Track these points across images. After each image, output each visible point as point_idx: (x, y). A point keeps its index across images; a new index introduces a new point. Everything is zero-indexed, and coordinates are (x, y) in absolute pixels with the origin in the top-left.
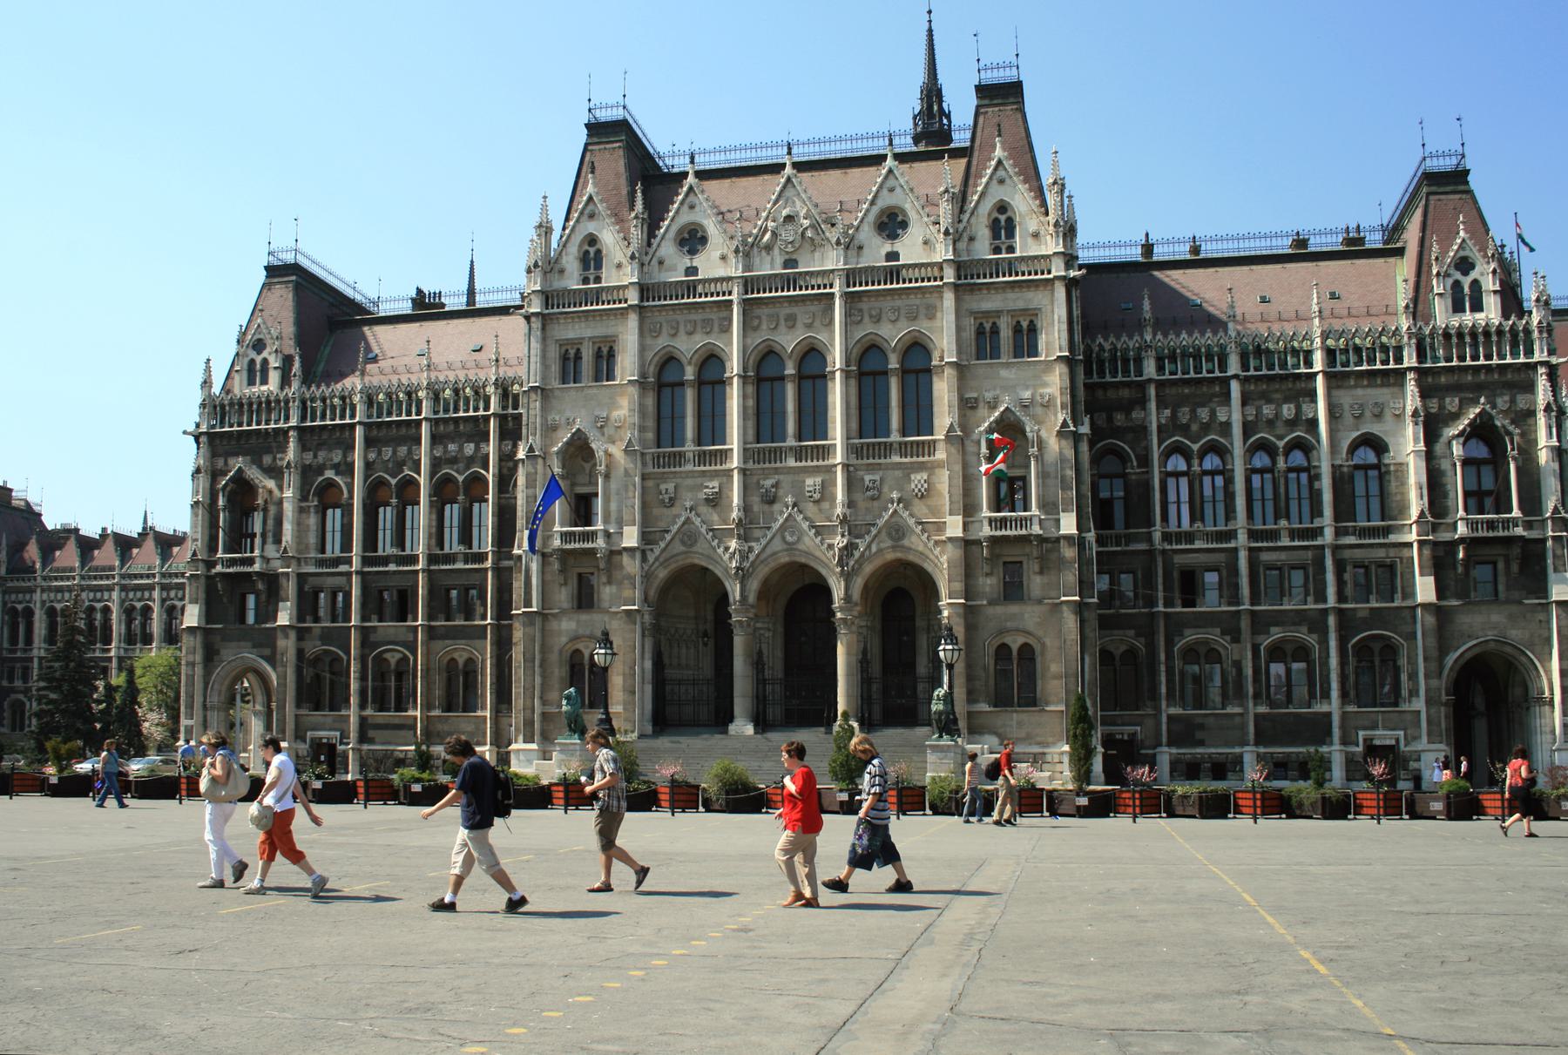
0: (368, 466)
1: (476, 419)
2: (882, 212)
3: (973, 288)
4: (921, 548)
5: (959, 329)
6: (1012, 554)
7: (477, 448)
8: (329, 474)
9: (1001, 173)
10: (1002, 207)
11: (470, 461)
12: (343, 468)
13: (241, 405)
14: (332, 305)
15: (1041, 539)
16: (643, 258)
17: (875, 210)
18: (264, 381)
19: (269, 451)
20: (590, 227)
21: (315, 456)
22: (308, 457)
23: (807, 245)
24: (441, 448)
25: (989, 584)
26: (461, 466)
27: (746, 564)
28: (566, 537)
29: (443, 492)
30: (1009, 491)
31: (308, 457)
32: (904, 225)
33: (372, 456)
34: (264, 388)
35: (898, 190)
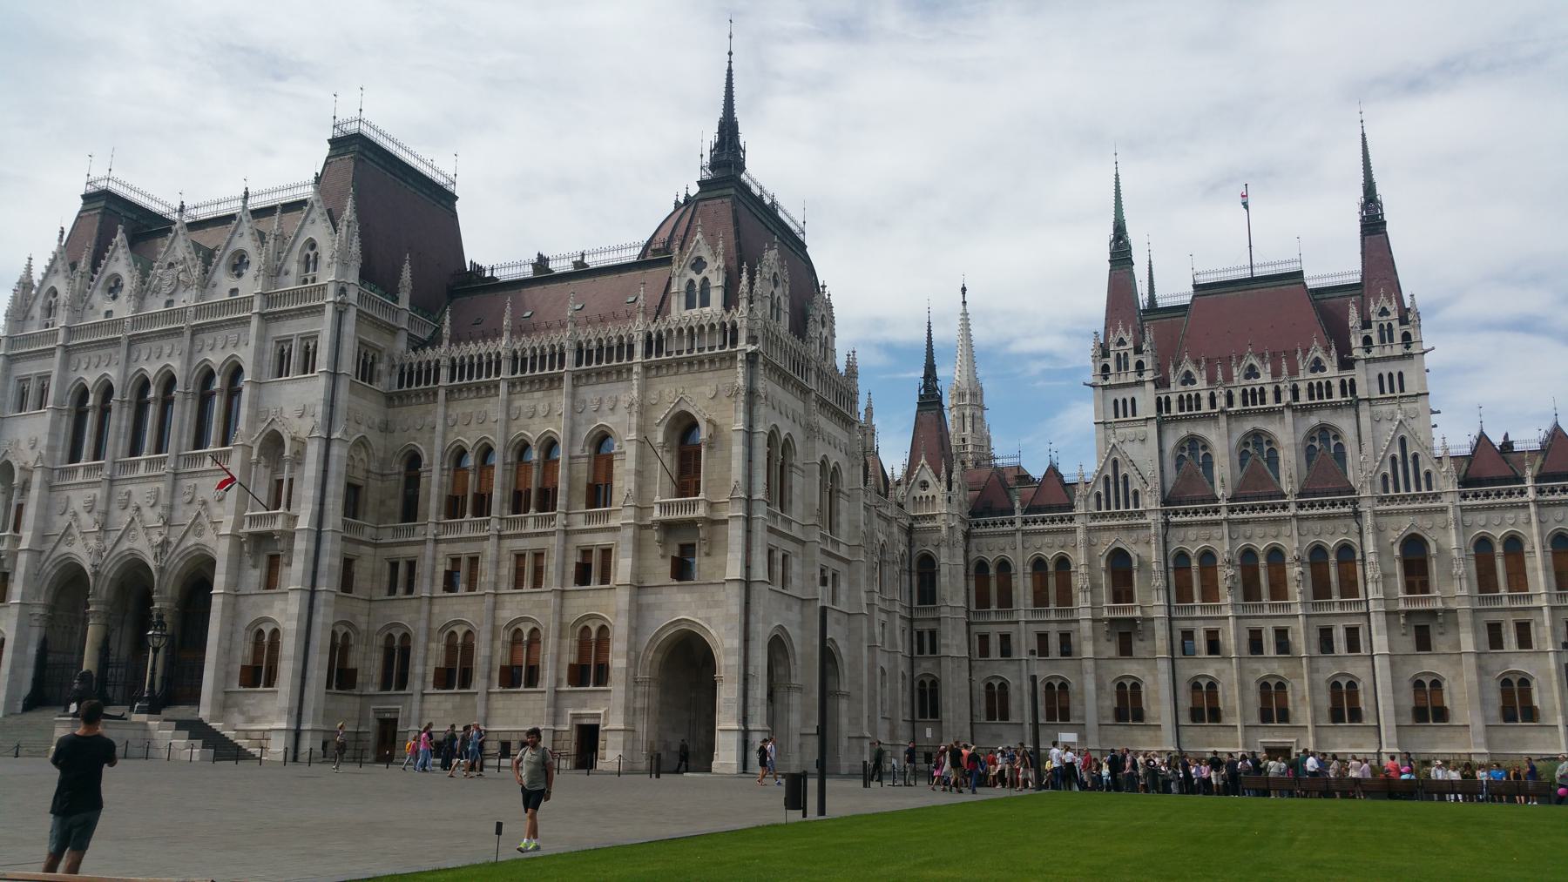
2: (235, 253)
10: (312, 244)
17: (229, 252)
25: (254, 576)
30: (279, 495)
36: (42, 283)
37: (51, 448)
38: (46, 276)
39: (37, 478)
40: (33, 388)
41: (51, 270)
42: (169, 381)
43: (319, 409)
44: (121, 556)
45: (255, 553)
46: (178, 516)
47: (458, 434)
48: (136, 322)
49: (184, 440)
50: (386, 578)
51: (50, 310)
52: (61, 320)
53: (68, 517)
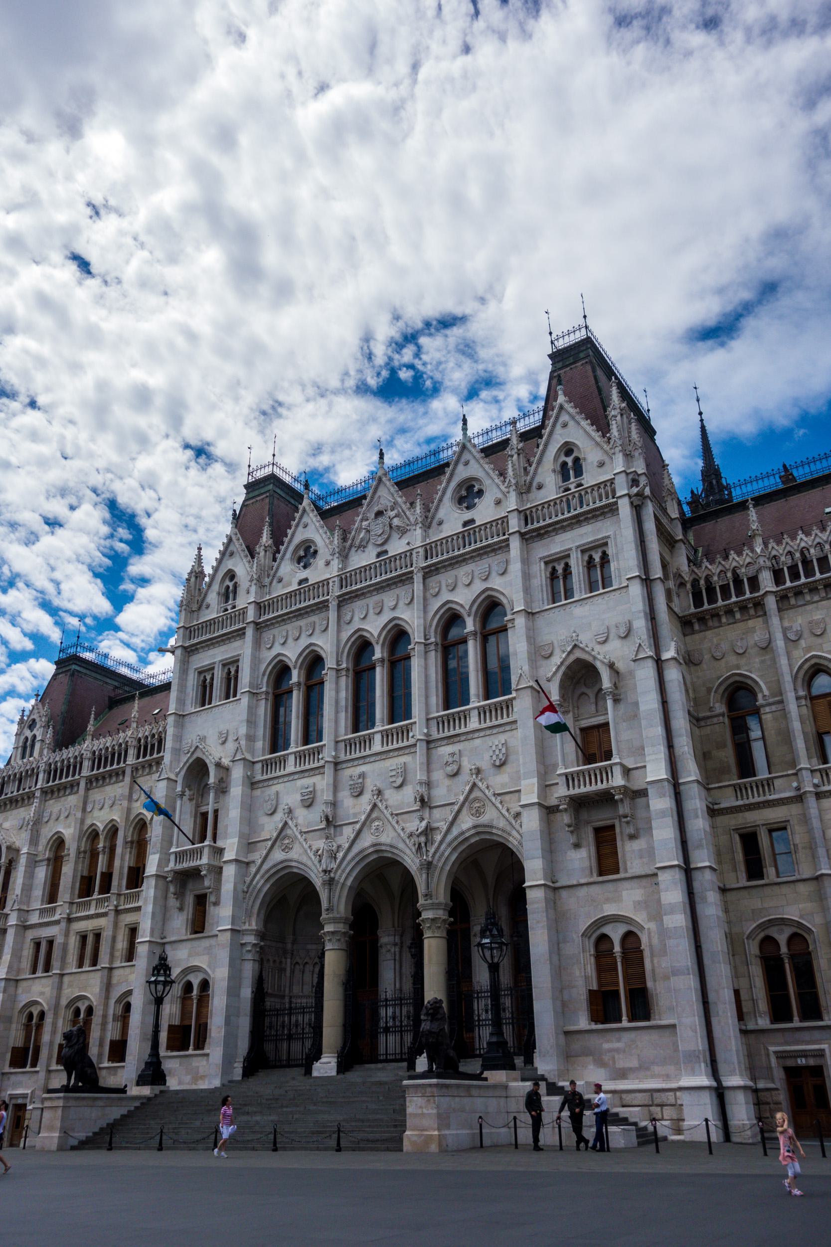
2: (460, 485)
3: (541, 534)
4: (502, 823)
5: (527, 576)
6: (601, 817)
9: (564, 418)
10: (568, 449)
14: (116, 687)
15: (625, 790)
16: (262, 581)
17: (453, 484)
20: (229, 564)
23: (395, 536)
27: (334, 865)
28: (180, 856)
32: (480, 493)
34: (31, 759)
35: (472, 462)
36: (216, 569)
37: (251, 738)
38: (220, 561)
39: (238, 773)
40: (219, 675)
41: (226, 553)
42: (398, 636)
43: (641, 625)
44: (363, 856)
45: (576, 827)
46: (441, 793)
47: (809, 649)
48: (343, 580)
49: (433, 700)
50: (740, 856)
51: (229, 594)
52: (245, 600)
53: (279, 817)
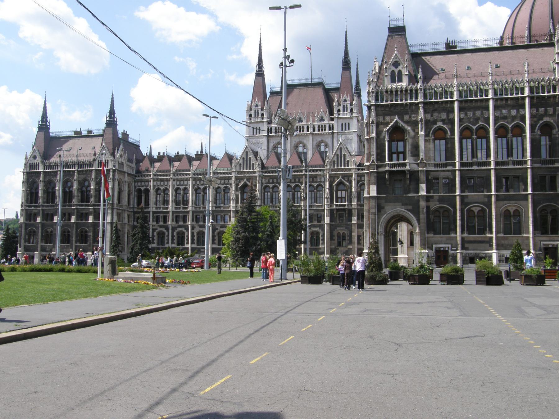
0: (460, 120)
1: (517, 98)
7: (518, 112)
8: (440, 124)
11: (514, 118)
12: (446, 121)
13: (391, 92)
18: (400, 80)
19: (407, 113)
21: (432, 116)
22: (429, 117)
24: (498, 112)
26: (509, 120)
29: (501, 132)
31: (429, 117)
33: (463, 116)
34: (400, 84)
